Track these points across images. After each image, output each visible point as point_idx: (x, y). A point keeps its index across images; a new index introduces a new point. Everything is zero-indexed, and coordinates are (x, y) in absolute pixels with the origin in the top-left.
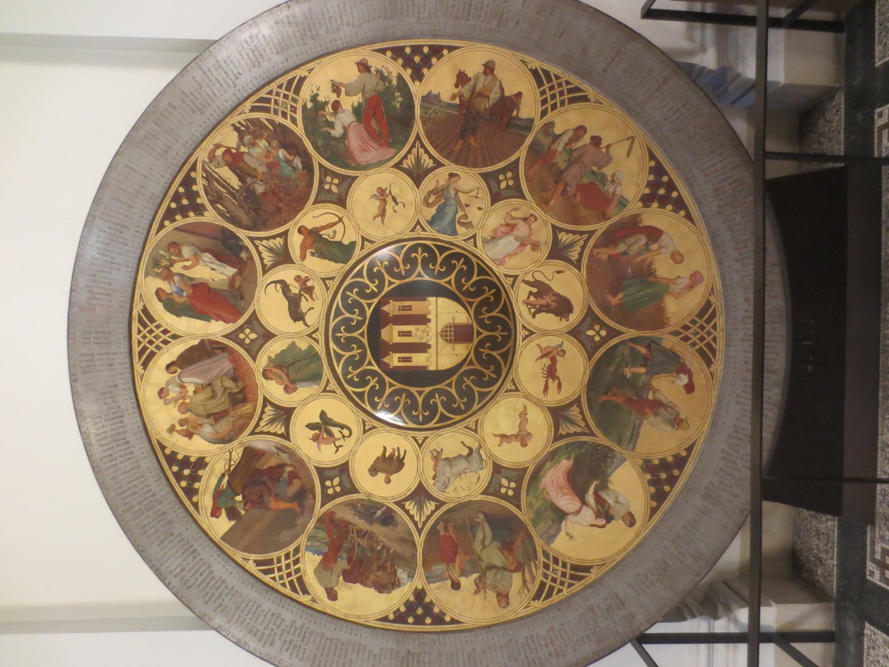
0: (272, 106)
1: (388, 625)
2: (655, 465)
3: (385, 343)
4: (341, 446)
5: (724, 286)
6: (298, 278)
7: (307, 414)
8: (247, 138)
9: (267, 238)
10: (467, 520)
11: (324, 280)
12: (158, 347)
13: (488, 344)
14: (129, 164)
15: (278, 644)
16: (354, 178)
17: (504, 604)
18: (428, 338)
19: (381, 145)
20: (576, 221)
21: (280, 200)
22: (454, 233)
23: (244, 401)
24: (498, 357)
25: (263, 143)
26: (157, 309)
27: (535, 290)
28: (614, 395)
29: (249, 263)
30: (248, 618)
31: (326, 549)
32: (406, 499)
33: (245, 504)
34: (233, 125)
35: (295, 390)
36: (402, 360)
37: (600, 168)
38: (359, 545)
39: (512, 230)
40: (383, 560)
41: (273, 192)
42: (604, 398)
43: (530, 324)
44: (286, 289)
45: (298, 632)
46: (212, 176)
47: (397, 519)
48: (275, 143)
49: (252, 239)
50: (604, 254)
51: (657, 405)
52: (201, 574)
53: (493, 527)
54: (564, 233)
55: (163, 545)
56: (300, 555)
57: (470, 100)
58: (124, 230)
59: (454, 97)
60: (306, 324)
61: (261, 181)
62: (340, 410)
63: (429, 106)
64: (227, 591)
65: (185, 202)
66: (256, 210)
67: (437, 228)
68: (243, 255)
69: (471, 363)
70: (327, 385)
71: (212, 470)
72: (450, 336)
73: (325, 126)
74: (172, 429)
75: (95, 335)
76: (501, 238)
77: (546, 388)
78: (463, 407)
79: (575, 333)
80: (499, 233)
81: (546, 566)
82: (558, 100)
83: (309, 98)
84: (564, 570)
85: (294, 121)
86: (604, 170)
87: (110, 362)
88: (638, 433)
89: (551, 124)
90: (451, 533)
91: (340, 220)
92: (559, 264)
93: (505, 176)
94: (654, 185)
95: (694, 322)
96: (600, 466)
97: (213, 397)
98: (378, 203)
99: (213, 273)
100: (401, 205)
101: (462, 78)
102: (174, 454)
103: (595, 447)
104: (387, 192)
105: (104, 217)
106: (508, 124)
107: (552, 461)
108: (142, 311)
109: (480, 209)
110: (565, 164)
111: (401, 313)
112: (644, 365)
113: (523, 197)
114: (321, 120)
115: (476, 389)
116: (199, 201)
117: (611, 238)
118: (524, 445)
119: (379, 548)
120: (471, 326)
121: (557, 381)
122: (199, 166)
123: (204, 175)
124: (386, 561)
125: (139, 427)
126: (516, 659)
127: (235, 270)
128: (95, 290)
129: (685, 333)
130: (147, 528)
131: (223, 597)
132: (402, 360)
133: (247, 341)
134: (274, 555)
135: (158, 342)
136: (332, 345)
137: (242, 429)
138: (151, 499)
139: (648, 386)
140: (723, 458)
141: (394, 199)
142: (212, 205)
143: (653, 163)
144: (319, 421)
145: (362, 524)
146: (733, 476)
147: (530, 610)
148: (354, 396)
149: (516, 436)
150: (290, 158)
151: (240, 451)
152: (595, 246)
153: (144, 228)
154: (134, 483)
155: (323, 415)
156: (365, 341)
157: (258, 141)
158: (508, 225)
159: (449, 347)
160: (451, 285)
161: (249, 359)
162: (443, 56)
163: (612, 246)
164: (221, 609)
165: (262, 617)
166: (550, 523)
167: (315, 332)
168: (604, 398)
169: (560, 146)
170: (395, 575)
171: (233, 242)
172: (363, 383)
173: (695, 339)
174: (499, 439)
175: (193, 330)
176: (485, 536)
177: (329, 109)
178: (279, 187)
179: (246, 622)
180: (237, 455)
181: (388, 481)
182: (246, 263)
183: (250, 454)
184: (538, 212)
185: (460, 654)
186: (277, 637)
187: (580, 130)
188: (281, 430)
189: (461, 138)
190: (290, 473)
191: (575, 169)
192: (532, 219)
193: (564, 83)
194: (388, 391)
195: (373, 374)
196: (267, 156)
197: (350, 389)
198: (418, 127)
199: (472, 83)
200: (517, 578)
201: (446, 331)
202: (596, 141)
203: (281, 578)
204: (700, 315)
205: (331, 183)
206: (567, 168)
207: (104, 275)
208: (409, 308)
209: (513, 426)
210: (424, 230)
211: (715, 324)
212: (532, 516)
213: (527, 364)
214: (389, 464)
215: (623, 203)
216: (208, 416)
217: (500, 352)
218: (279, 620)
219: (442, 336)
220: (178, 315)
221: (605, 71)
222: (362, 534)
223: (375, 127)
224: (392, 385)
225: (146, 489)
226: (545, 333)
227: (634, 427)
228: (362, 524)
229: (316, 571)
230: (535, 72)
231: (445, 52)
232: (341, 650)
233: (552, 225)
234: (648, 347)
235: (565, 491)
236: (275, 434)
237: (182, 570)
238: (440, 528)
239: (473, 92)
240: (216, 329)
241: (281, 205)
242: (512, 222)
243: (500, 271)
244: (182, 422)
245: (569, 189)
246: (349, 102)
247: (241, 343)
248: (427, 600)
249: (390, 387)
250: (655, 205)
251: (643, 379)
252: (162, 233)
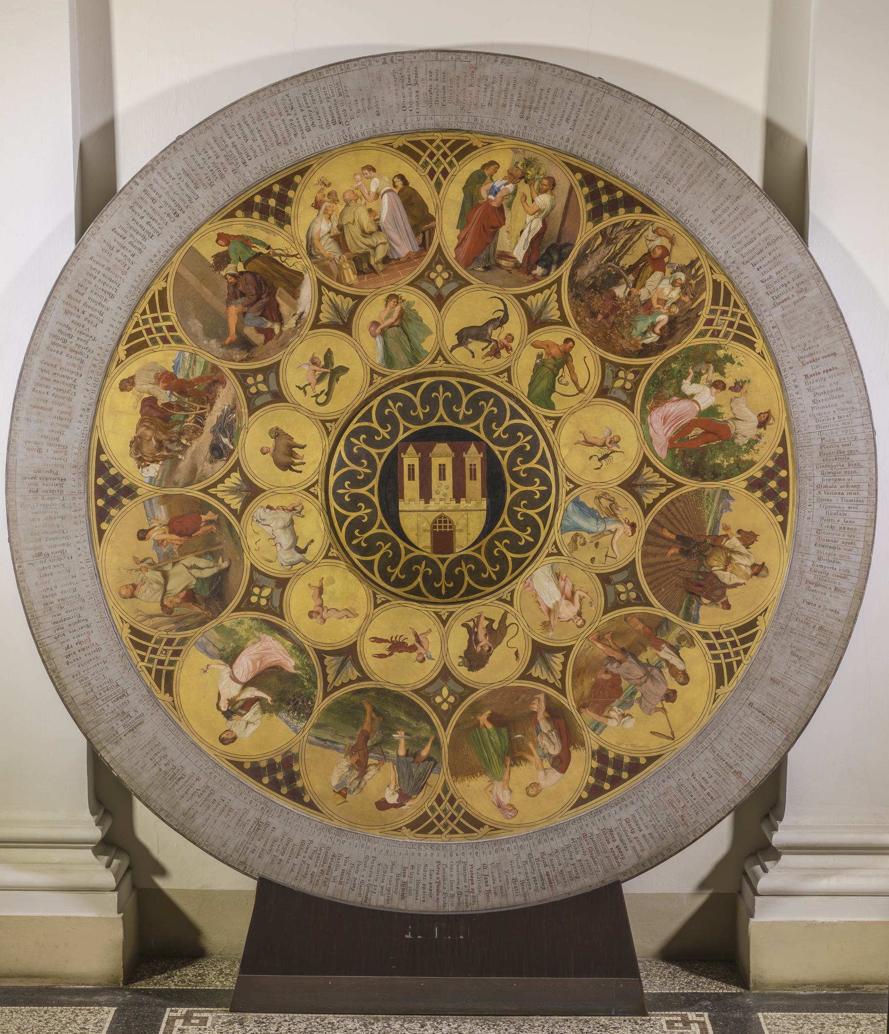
0: (721, 308)
1: (94, 453)
2: (292, 766)
3: (431, 449)
4: (305, 393)
5: (501, 842)
7: (344, 352)
8: (681, 276)
9: (559, 300)
10: (219, 548)
11: (508, 370)
12: (426, 163)
13: (430, 572)
14: (652, 128)
15: (67, 320)
16: (631, 408)
17: (123, 592)
18: (437, 501)
19: (671, 440)
20: (578, 674)
21: (606, 317)
22: (564, 530)
23: (360, 272)
24: (415, 584)
25: (675, 294)
26: (473, 165)
27: (495, 626)
28: (372, 719)
29: (530, 278)
30: (94, 282)
31: (180, 376)
32: (243, 474)
33: (233, 275)
34: (698, 259)
35: (374, 336)
36: (411, 468)
37: (640, 701)
38: (187, 416)
39: (566, 598)
40: (169, 446)
41: (615, 308)
42: (368, 708)
43: (455, 620)
44: (498, 323)
45: (82, 344)
46: (636, 233)
47: (219, 464)
48: (676, 310)
49: (558, 281)
50: (539, 706)
51: (362, 768)
52: (148, 223)
53: (214, 577)
54: (563, 659)
55: (183, 176)
56: (173, 344)
57: (723, 548)
58: (571, 123)
59: (727, 528)
61: (630, 293)
62: (349, 392)
64: (129, 256)
65: (605, 199)
66: (593, 286)
67: (570, 508)
68: (539, 270)
69: (408, 552)
70: (379, 374)
71: (275, 234)
72: (440, 527)
73: (695, 372)
75: (441, 87)
76: (558, 586)
78: (355, 542)
79: (445, 674)
80: (563, 583)
81: (170, 642)
82: (720, 651)
83: (729, 353)
84: (166, 663)
85: (702, 334)
86: (636, 705)
87: (408, 105)
88: (328, 747)
89: (692, 644)
90: (204, 529)
91: (581, 391)
92: (526, 654)
93: (631, 591)
94: (618, 763)
95: (459, 809)
96: (289, 704)
97: (365, 234)
99: (515, 240)
100: (599, 464)
101: (748, 538)
102: (295, 187)
103: (311, 698)
104: (615, 448)
105: (587, 97)
106: (693, 593)
107: (293, 648)
108: (471, 145)
109: (593, 560)
110: (644, 661)
111: (467, 467)
112: (407, 755)
113: (606, 612)
114: (703, 367)
115: (377, 557)
116: (606, 215)
117: (556, 713)
118: (311, 615)
119: (184, 442)
120: (451, 551)
121: (387, 653)
122: (648, 217)
123: (638, 223)
124: (168, 450)
125: (327, 144)
126: (61, 608)
127: (520, 260)
128: (496, 86)
129: (446, 799)
130: (204, 156)
131: (122, 250)
132: (411, 468)
133: (433, 275)
134: (172, 312)
135: (431, 164)
136: (428, 381)
137: (326, 270)
138: (240, 160)
139: (384, 758)
140: (303, 843)
141: (605, 456)
142: (601, 231)
143: (643, 761)
144: (335, 366)
145: (212, 420)
146: (283, 854)
147: (119, 624)
148: (366, 408)
149: (321, 605)
150: (657, 329)
151: (299, 268)
152: (548, 697)
153: (572, 149)
154: (259, 139)
155: (344, 370)
156: (433, 423)
157: (678, 290)
158: (573, 593)
159: (426, 525)
160: (501, 526)
161: (410, 278)
162: (776, 515)
163: (547, 715)
164: (107, 248)
165: (98, 299)
166: (221, 646)
167: (445, 359)
168: (368, 708)
169: (666, 654)
170: (152, 462)
171: (556, 257)
172: (384, 420)
173: (439, 810)
174: (317, 584)
175: (448, 208)
176: (202, 569)
177: (716, 377)
178: (622, 315)
179: (92, 280)
180: (290, 263)
182: (529, 273)
184: (589, 630)
185: (65, 541)
186: (75, 319)
187: (684, 678)
188: (324, 318)
189: (678, 537)
190: (272, 330)
191: (638, 672)
192: (579, 623)
193: (739, 658)
194: (373, 452)
195: (394, 434)
196: (659, 300)
197: (375, 403)
198: (691, 485)
199: (743, 549)
200: (156, 608)
201: (445, 522)
202: (671, 696)
203: (145, 322)
204: (467, 816)
205: (625, 379)
206: (639, 662)
207: (515, 99)
208: (473, 477)
209: (333, 605)
210: (568, 493)
211: (457, 833)
212: (227, 624)
213: (410, 618)
214: (286, 455)
215: (597, 727)
216: (341, 228)
217: (422, 585)
218: (95, 321)
219: (440, 517)
221: (751, 704)
222: (200, 420)
223: (693, 433)
224: (380, 456)
225: (251, 153)
226: (444, 641)
227: (333, 742)
228: (212, 420)
230: (753, 624)
231: (780, 518)
232: (63, 398)
233: (573, 646)
234: (429, 758)
235: (258, 663)
236: (319, 311)
237: (153, 199)
238: (210, 516)
239: (732, 551)
241: (600, 317)
242: (577, 598)
243: (518, 586)
245: (615, 665)
247: (430, 267)
248: (125, 501)
249: (378, 454)
250: (595, 764)
251: (392, 753)
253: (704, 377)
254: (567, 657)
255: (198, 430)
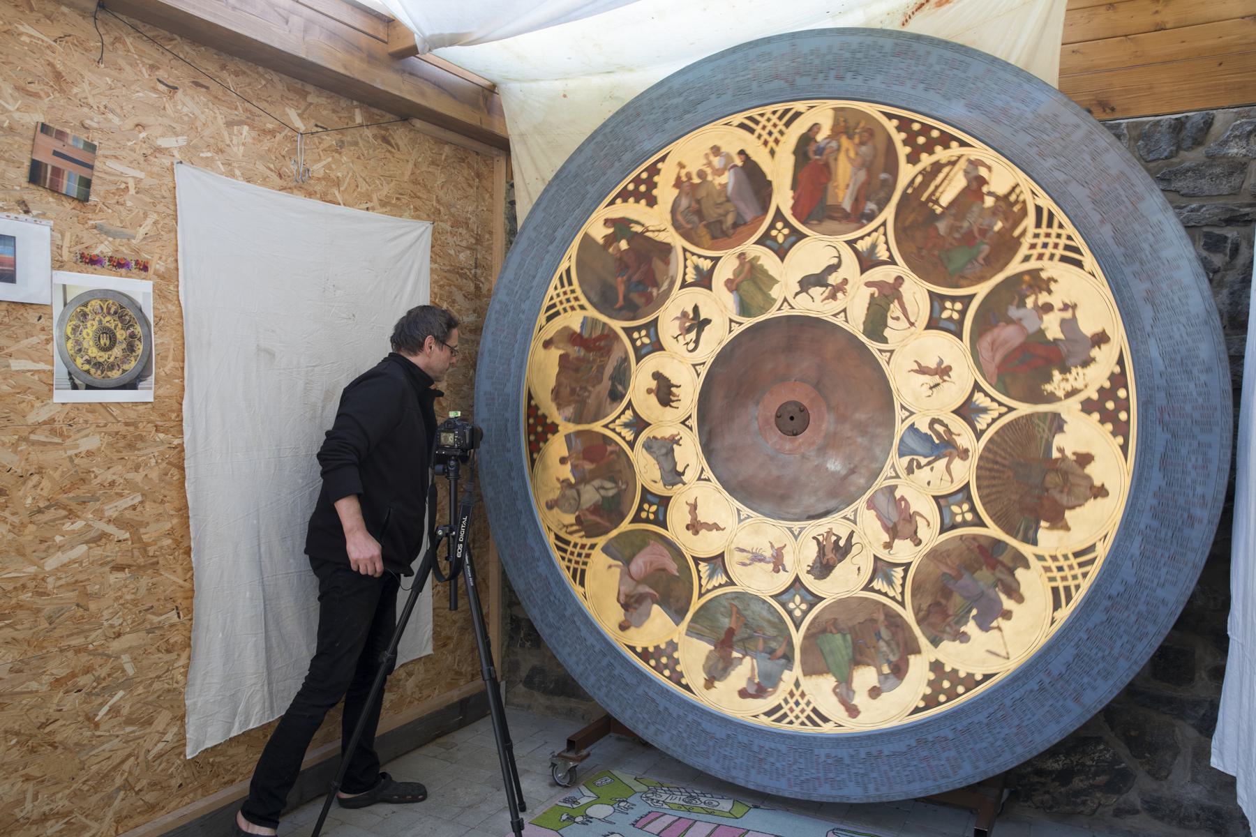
6: (845, 281)
11: (844, 310)
23: (714, 238)
26: (799, 128)
27: (842, 543)
34: (1017, 185)
35: (731, 290)
60: (797, 294)
62: (714, 340)
63: (1048, 422)
74: (681, 166)
77: (743, 550)
85: (1027, 258)
91: (912, 324)
98: (933, 365)
109: (929, 483)
113: (942, 531)
122: (964, 150)
141: (937, 385)
145: (609, 370)
149: (694, 518)
155: (707, 321)
180: (661, 237)
181: (649, 391)
183: (666, 249)
184: (925, 548)
188: (689, 279)
190: (651, 293)
198: (1024, 409)
200: (570, 519)
220: (795, 153)
222: (602, 368)
228: (609, 370)
229: (566, 328)
236: (685, 274)
240: (783, 198)
244: (689, 176)
246: (1052, 327)
252: (884, 120)
253: (1030, 302)
254: (906, 571)
255: (599, 379)
